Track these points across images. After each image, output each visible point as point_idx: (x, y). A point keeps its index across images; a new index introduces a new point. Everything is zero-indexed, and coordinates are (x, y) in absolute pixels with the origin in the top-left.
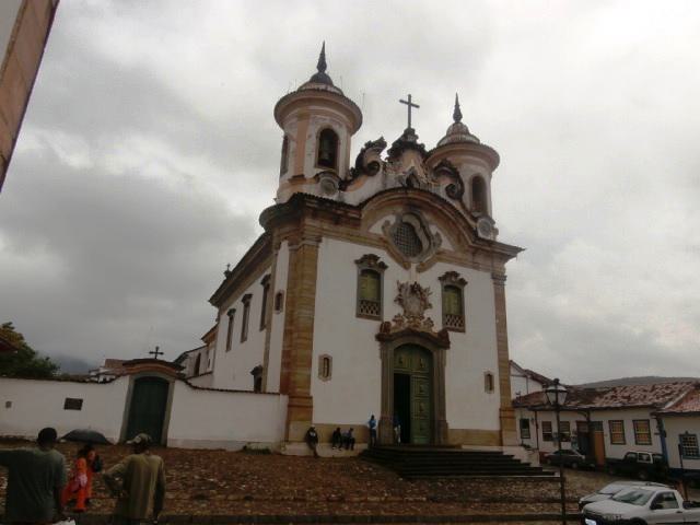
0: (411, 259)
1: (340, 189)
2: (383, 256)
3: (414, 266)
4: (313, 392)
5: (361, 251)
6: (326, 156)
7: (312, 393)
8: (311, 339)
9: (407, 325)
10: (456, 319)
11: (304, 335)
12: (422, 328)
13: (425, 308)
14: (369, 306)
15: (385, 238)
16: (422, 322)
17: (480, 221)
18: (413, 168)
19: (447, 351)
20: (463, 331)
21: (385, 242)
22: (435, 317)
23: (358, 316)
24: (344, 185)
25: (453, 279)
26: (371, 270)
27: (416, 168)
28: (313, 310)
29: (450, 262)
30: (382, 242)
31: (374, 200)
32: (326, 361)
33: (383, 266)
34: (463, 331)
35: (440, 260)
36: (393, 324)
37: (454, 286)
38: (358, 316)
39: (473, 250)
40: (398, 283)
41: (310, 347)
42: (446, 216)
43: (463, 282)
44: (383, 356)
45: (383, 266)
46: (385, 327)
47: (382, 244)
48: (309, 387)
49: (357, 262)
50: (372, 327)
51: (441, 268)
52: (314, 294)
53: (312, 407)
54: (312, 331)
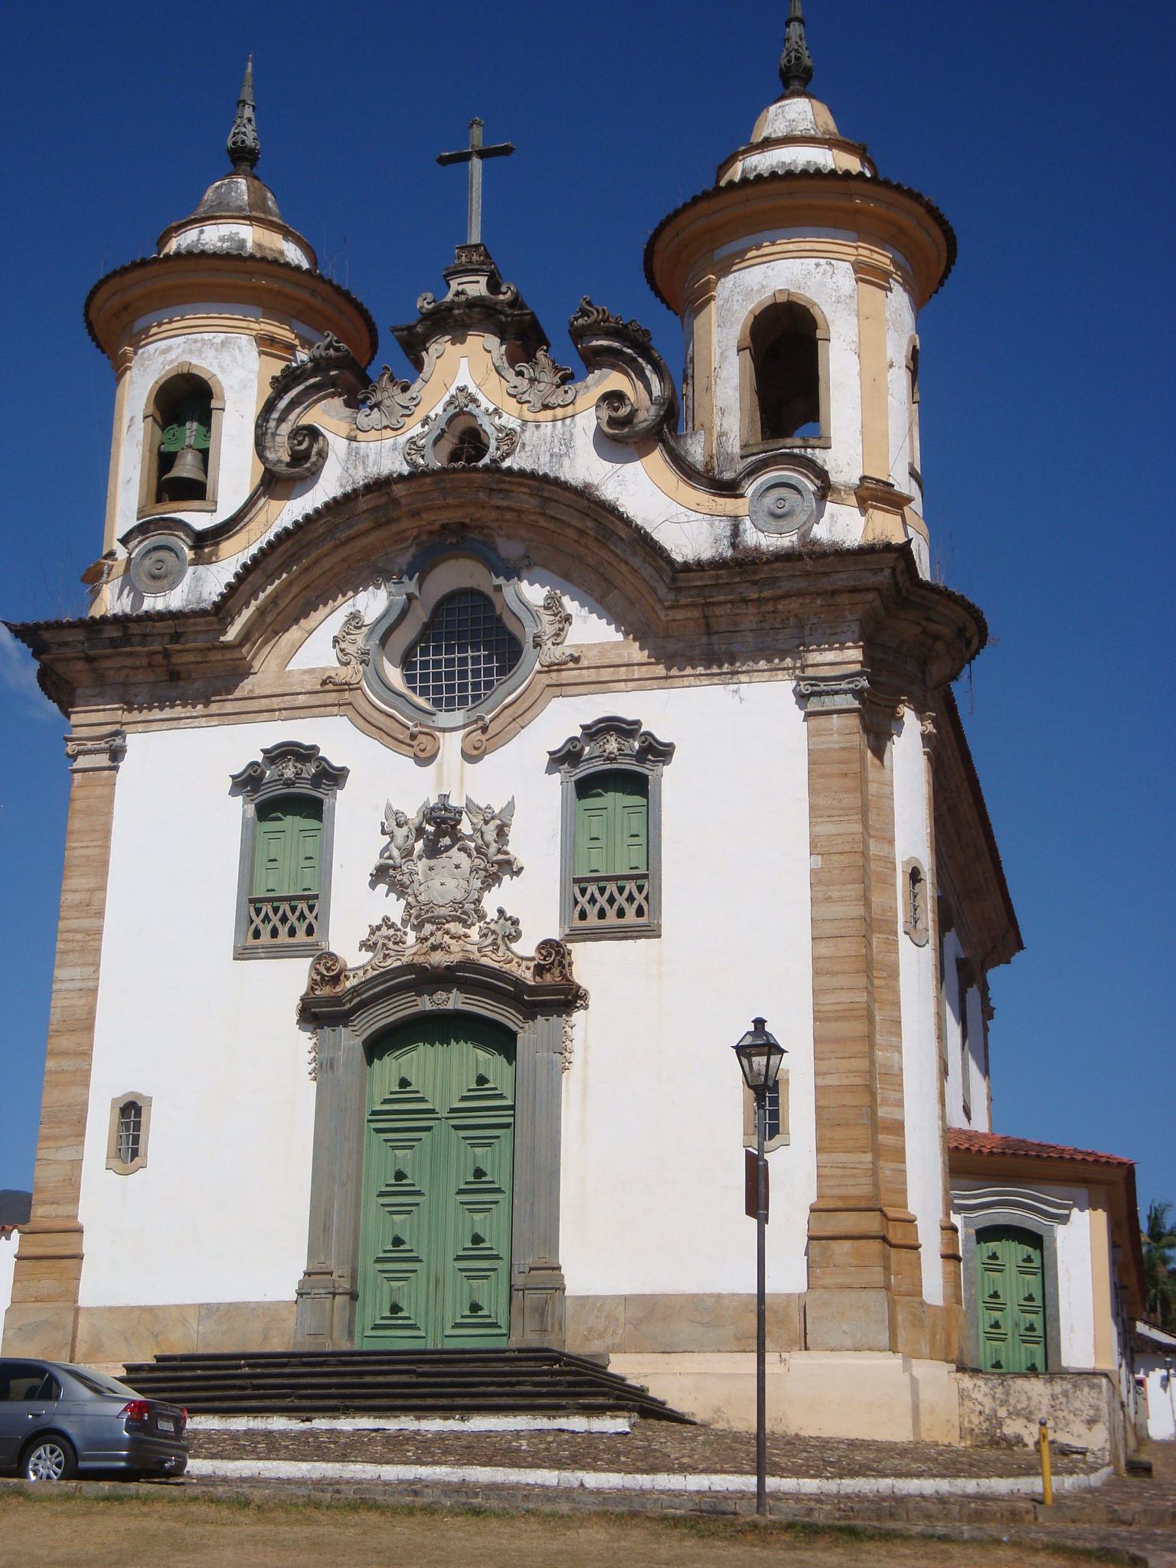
0: (444, 719)
1: (195, 562)
2: (334, 738)
3: (451, 745)
4: (86, 1214)
5: (245, 742)
6: (186, 467)
7: (82, 1219)
8: (86, 1054)
9: (405, 960)
10: (617, 898)
11: (65, 1042)
12: (469, 943)
13: (491, 879)
14: (278, 916)
15: (344, 674)
16: (474, 933)
17: (750, 489)
18: (462, 389)
19: (578, 1016)
20: (652, 932)
21: (346, 687)
22: (532, 905)
23: (242, 953)
24: (206, 542)
25: (612, 745)
26: (290, 794)
27: (472, 389)
28: (96, 965)
29: (601, 686)
30: (332, 694)
31: (272, 563)
32: (131, 1113)
33: (335, 777)
34: (652, 932)
35: (560, 689)
36: (353, 956)
37: (615, 772)
38: (242, 953)
39: (696, 613)
40: (389, 807)
41: (83, 1078)
42: (570, 525)
43: (658, 752)
44: (323, 1068)
45: (335, 777)
46: (328, 971)
47: (332, 698)
48: (76, 1200)
49: (233, 777)
50: (293, 977)
51: (562, 719)
52: (100, 914)
53: (80, 1257)
54: (90, 1028)
